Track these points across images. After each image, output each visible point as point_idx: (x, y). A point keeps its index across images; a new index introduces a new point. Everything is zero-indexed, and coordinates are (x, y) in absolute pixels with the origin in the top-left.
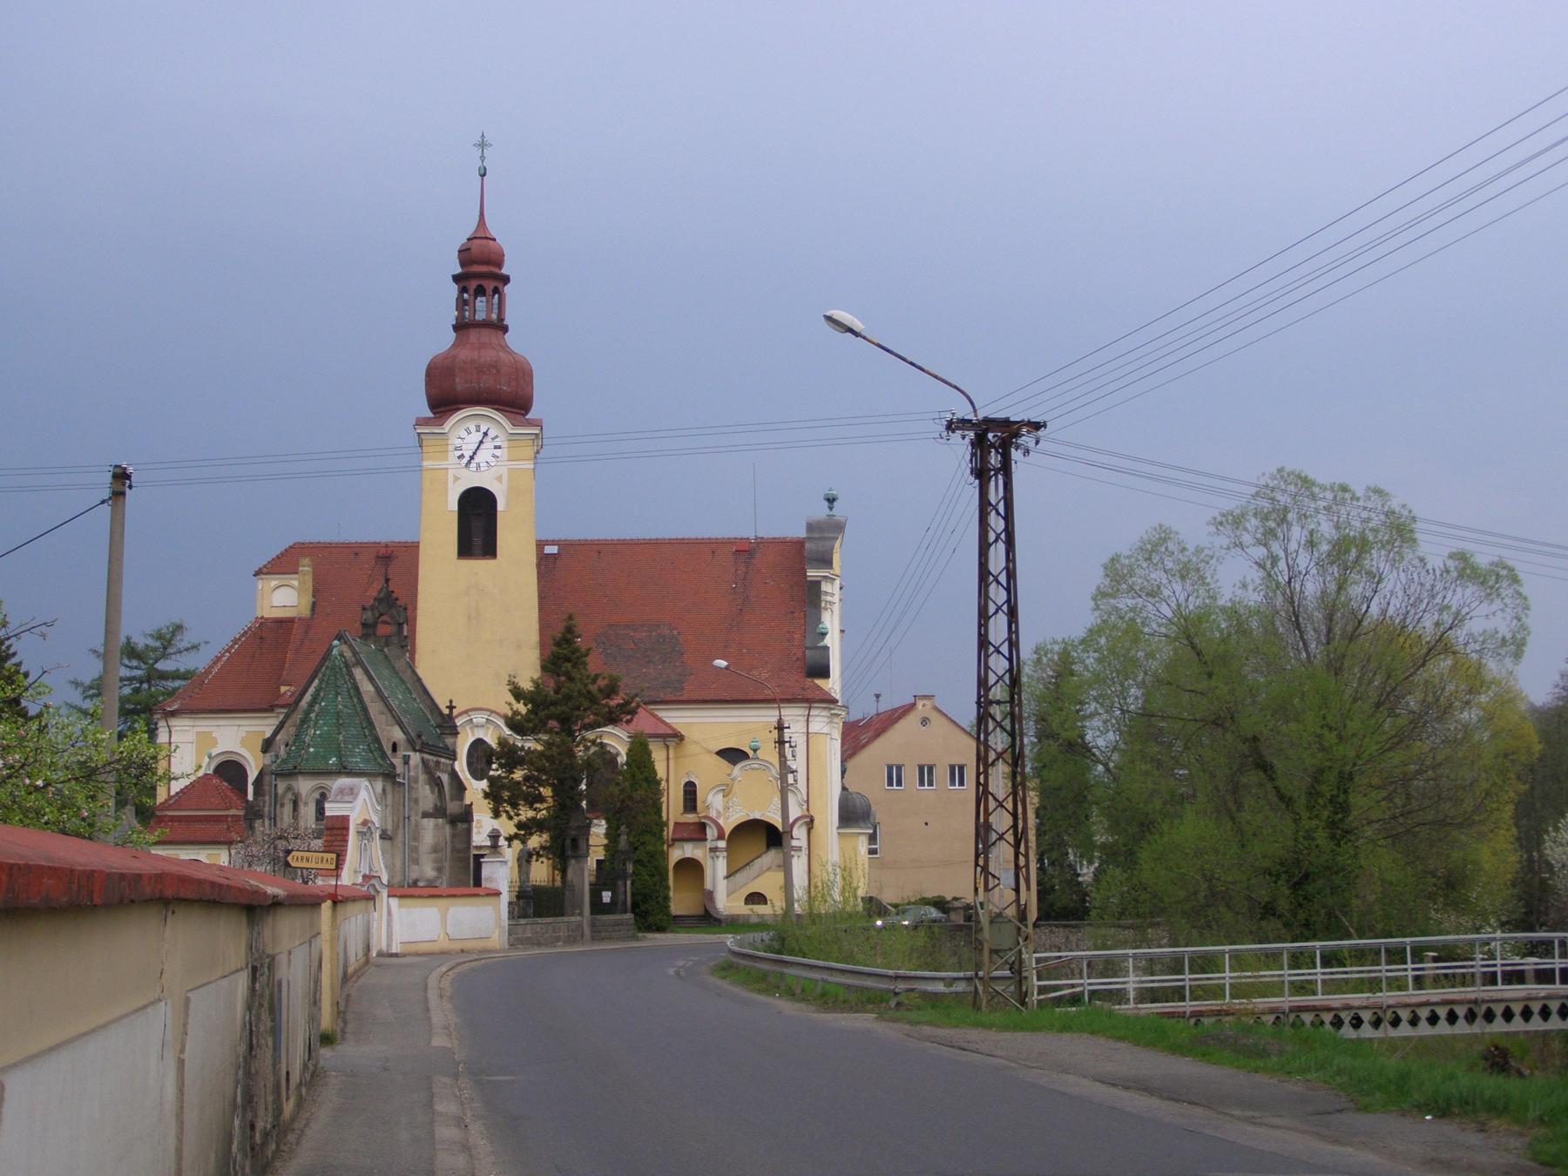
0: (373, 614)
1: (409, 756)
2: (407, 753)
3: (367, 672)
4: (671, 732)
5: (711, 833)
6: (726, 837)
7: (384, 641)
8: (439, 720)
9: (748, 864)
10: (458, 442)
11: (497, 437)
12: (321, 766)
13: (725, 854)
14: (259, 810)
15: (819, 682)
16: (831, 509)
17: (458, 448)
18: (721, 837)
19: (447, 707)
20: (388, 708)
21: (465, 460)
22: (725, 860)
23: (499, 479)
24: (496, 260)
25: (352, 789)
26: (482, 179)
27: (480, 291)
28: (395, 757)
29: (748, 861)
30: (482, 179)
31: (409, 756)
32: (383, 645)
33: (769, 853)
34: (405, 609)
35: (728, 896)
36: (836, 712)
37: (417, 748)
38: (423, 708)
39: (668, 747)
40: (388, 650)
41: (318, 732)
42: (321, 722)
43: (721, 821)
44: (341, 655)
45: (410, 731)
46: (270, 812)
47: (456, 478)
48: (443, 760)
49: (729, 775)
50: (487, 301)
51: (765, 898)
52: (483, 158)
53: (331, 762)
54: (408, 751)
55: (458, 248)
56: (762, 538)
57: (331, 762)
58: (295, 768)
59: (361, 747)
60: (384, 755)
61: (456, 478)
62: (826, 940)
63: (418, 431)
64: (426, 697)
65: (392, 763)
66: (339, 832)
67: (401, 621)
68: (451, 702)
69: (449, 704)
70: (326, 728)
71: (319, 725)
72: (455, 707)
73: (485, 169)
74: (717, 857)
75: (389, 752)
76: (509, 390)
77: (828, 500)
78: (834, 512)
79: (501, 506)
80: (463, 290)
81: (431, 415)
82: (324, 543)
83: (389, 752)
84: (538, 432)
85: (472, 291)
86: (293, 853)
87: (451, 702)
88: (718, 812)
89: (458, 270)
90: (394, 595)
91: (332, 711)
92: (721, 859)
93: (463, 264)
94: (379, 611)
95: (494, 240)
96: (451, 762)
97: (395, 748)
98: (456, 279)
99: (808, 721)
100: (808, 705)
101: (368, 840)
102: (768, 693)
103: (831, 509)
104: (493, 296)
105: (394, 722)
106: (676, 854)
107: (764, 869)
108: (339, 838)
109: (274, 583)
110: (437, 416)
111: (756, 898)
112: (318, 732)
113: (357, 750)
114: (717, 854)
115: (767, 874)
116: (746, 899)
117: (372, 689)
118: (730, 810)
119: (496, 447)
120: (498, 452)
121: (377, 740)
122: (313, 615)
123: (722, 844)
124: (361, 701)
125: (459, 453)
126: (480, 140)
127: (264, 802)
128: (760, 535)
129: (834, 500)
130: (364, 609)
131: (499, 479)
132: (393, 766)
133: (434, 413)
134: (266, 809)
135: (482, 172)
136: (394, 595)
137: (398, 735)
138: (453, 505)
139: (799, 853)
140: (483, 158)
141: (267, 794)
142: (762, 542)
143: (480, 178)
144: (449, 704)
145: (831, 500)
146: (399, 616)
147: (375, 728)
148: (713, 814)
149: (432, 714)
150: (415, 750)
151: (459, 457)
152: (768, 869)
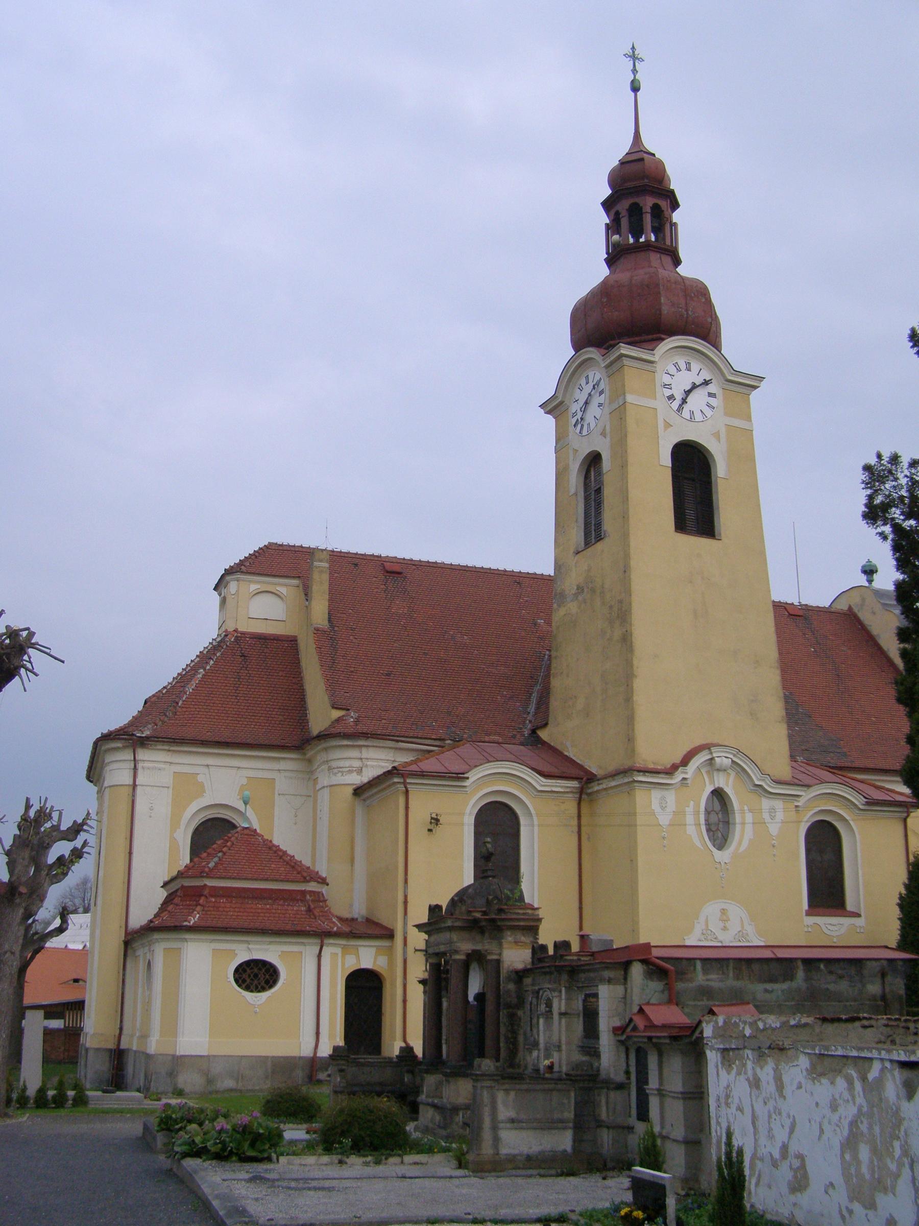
10: (667, 379)
21: (675, 405)
23: (717, 435)
47: (668, 425)
52: (634, 71)
109: (254, 587)
120: (712, 401)
140: (634, 71)
143: (632, 94)
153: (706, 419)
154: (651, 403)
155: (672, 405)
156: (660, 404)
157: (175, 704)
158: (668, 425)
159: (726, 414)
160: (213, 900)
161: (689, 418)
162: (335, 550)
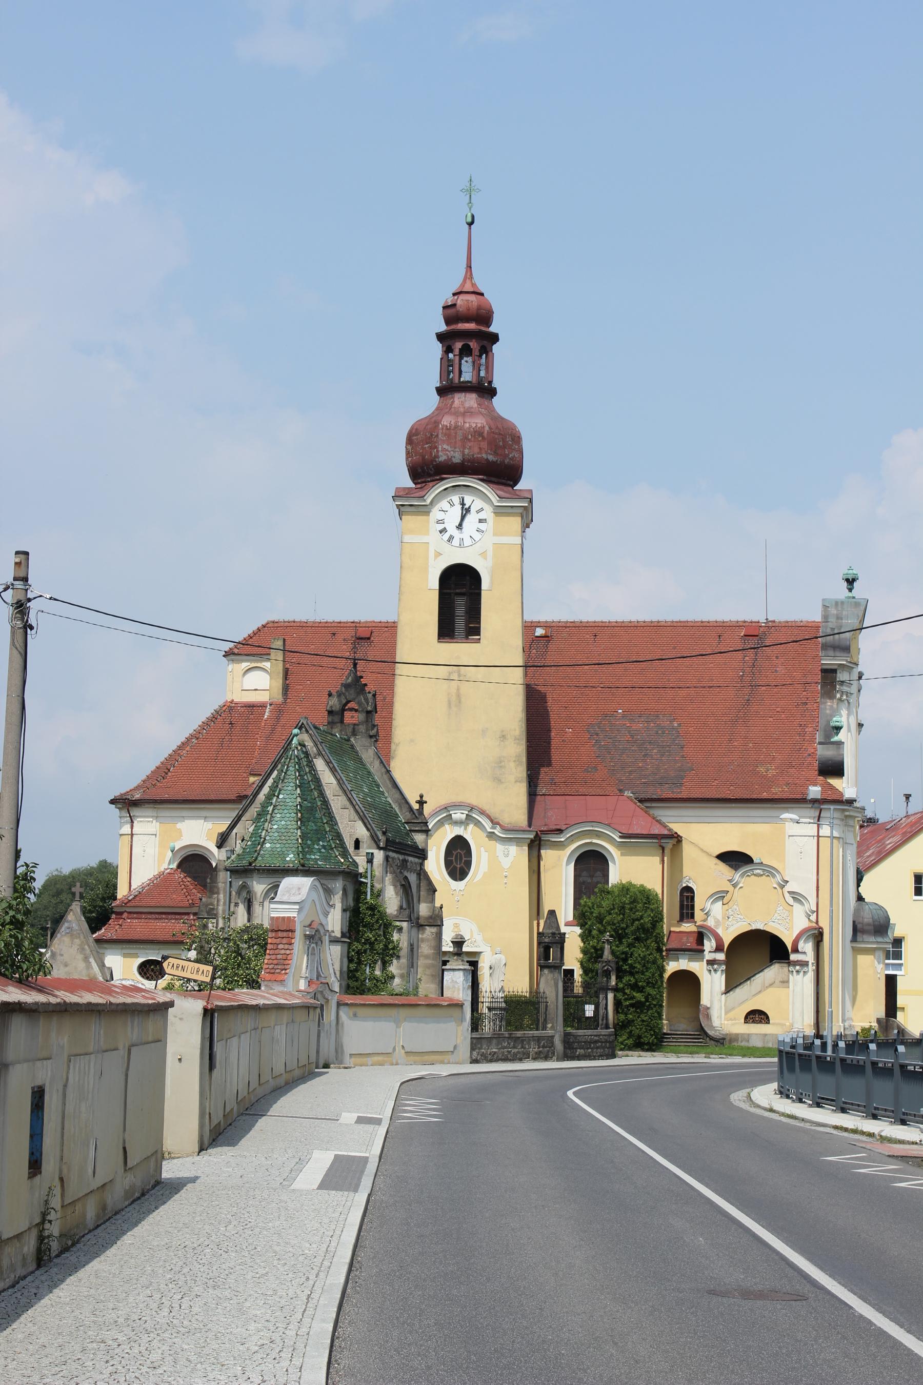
0: (340, 701)
1: (372, 854)
2: (371, 851)
3: (328, 763)
4: (666, 832)
5: (709, 945)
6: (725, 950)
7: (351, 730)
8: (408, 815)
9: (749, 979)
10: (440, 516)
11: (482, 509)
12: (277, 863)
13: (724, 967)
14: (213, 909)
15: (834, 782)
16: (850, 590)
17: (439, 522)
18: (719, 949)
19: (417, 802)
20: (351, 803)
22: (724, 976)
23: (483, 554)
24: (484, 317)
25: (299, 889)
26: (470, 228)
27: (466, 351)
28: (357, 855)
30: (470, 228)
31: (372, 854)
32: (349, 734)
33: (772, 967)
34: (374, 695)
35: (726, 1013)
36: (852, 814)
37: (382, 845)
38: (391, 802)
39: (663, 849)
40: (355, 739)
41: (275, 827)
42: (278, 815)
43: (720, 931)
44: (302, 745)
45: (373, 825)
46: (224, 911)
48: (410, 859)
49: (730, 881)
50: (474, 362)
51: (768, 1017)
53: (288, 859)
54: (370, 848)
55: (442, 304)
56: (774, 622)
57: (288, 859)
58: (250, 864)
59: (321, 843)
60: (345, 853)
61: (438, 554)
63: (397, 503)
64: (394, 790)
65: (354, 861)
66: (285, 934)
67: (369, 708)
68: (421, 796)
69: (419, 799)
70: (283, 823)
71: (276, 819)
72: (426, 802)
73: (473, 217)
74: (715, 971)
75: (351, 848)
76: (495, 459)
77: (847, 580)
78: (854, 593)
79: (485, 585)
80: (448, 350)
81: (412, 485)
82: (300, 622)
83: (351, 848)
84: (527, 505)
85: (457, 352)
86: (170, 960)
87: (421, 796)
88: (718, 922)
89: (443, 327)
90: (363, 681)
91: (291, 804)
92: (719, 973)
93: (448, 321)
94: (346, 698)
95: (482, 294)
96: (420, 861)
97: (357, 845)
98: (441, 337)
101: (316, 943)
102: (776, 791)
103: (850, 590)
104: (480, 356)
105: (357, 818)
106: (672, 967)
107: (767, 985)
108: (285, 941)
109: (245, 665)
110: (419, 486)
111: (757, 1016)
112: (275, 827)
113: (316, 847)
114: (715, 966)
115: (770, 989)
116: (746, 1017)
117: (334, 781)
118: (730, 920)
119: (481, 521)
120: (482, 526)
121: (339, 836)
122: (285, 699)
123: (721, 956)
124: (322, 794)
125: (441, 527)
126: (468, 185)
127: (218, 901)
128: (770, 619)
129: (854, 580)
130: (330, 695)
131: (483, 554)
132: (355, 864)
133: (415, 484)
134: (220, 908)
135: (469, 220)
136: (363, 681)
137: (361, 831)
138: (435, 584)
139: (805, 969)
141: (221, 892)
142: (772, 626)
144: (419, 799)
145: (850, 582)
146: (368, 704)
147: (336, 824)
148: (711, 923)
149: (400, 807)
150: (380, 848)
151: (441, 532)
152: (771, 985)
153: (474, 542)
154: (425, 539)
155: (443, 537)
156: (434, 539)
157: (166, 771)
158: (438, 554)
159: (495, 534)
160: (129, 921)
161: (458, 546)
162: (322, 621)
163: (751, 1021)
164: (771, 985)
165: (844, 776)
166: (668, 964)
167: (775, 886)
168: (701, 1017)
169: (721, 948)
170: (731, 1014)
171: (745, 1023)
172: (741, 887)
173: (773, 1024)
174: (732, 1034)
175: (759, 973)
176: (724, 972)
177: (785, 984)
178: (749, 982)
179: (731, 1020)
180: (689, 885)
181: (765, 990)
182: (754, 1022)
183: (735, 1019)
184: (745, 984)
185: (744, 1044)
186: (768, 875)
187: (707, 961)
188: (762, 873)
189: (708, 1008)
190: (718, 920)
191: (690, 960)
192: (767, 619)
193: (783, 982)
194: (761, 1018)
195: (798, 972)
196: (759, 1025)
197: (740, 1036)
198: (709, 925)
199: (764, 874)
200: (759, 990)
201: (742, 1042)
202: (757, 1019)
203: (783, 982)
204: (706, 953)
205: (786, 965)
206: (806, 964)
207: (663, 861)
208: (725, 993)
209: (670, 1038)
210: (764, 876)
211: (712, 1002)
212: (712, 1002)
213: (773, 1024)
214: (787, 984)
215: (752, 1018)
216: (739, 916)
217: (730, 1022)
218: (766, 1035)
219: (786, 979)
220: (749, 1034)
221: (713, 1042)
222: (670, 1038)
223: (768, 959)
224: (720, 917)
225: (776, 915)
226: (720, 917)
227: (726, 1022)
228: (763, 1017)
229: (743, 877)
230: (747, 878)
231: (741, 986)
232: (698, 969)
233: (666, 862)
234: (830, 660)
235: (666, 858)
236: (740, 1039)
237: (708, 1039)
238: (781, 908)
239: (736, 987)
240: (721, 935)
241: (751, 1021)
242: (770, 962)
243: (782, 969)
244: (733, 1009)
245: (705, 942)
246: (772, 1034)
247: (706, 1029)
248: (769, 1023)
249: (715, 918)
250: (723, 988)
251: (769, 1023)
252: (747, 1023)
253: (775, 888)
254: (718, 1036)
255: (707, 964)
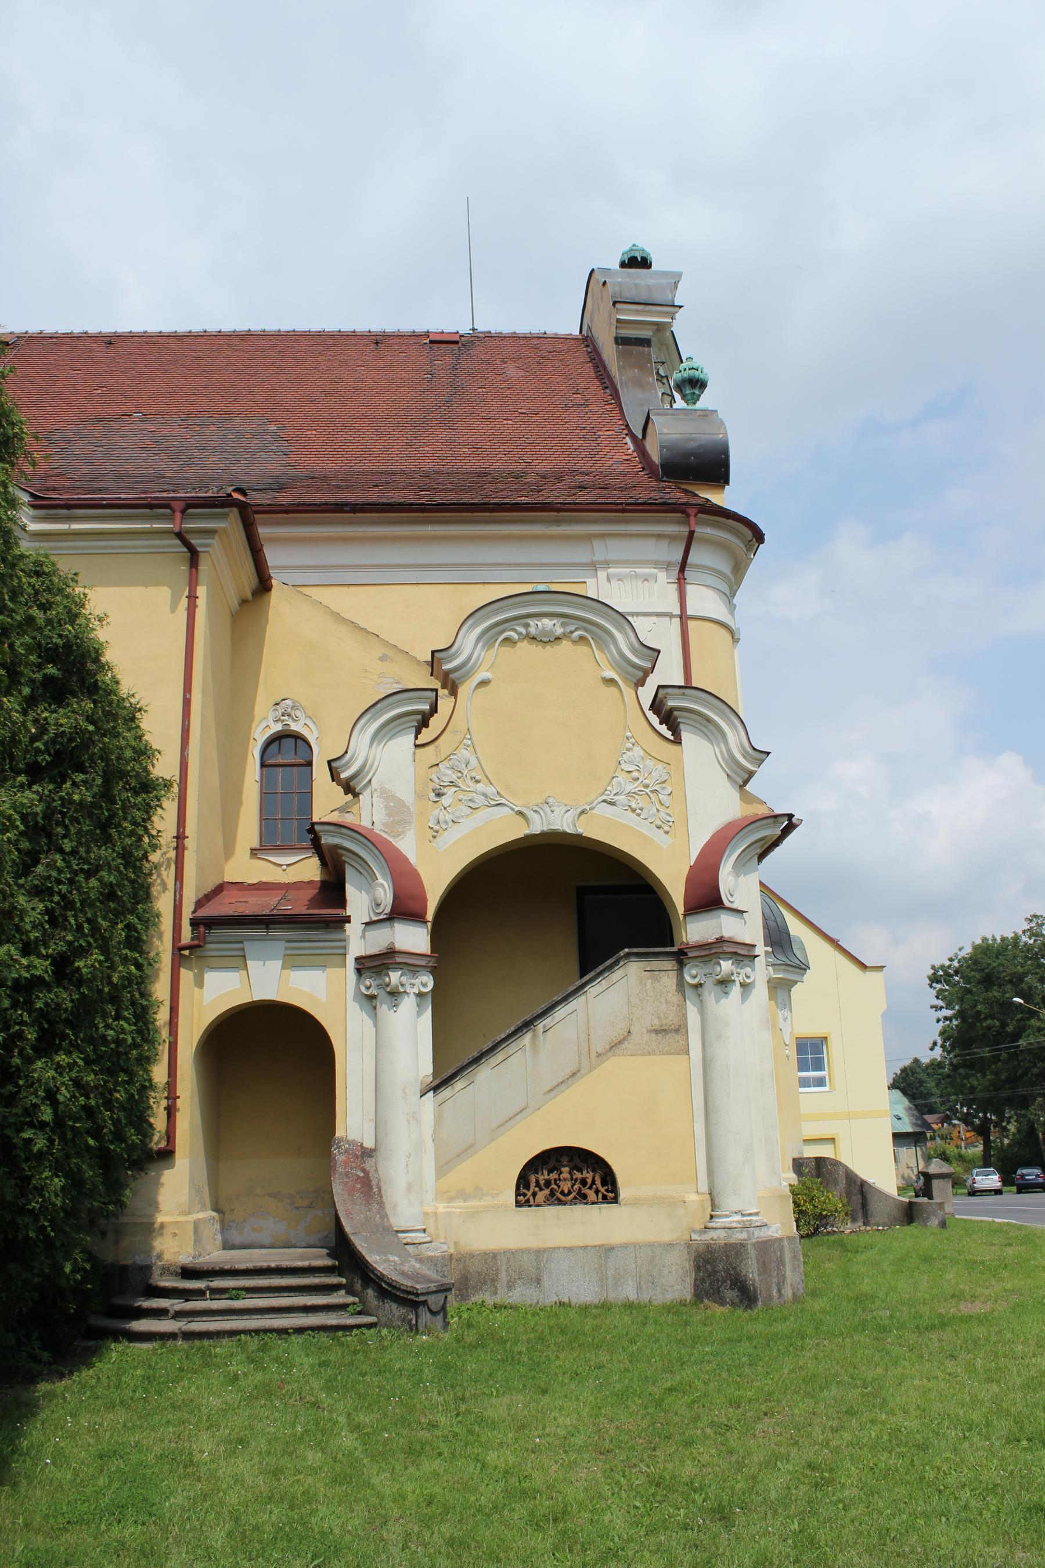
6: (430, 916)
9: (527, 1025)
13: (427, 982)
29: (528, 1017)
35: (442, 1169)
39: (194, 557)
43: (408, 846)
51: (609, 1178)
62: (830, 1316)
74: (395, 994)
88: (398, 811)
92: (408, 1003)
99: (682, 569)
100: (684, 530)
107: (599, 1046)
114: (395, 977)
115: (614, 1064)
116: (523, 1181)
118: (445, 801)
139: (741, 974)
152: (615, 1046)
163: (541, 1195)
164: (615, 1046)
165: (727, 482)
166: (200, 983)
167: (610, 674)
168: (338, 1189)
169: (414, 906)
170: (462, 1174)
171: (518, 1204)
172: (484, 683)
173: (636, 1202)
174: (472, 1256)
175: (565, 999)
176: (429, 998)
177: (672, 1039)
178: (527, 1039)
179: (462, 1195)
180: (294, 727)
181: (591, 1069)
182: (556, 1199)
183: (478, 1192)
184: (513, 1048)
185: (520, 1295)
186: (582, 638)
187: (358, 959)
188: (559, 631)
189: (368, 1153)
190: (401, 803)
191: (292, 961)
192: (473, 329)
193: (661, 1031)
194: (584, 1182)
195: (724, 983)
196: (579, 1211)
197: (502, 1263)
198: (366, 823)
199: (565, 636)
200: (568, 1071)
201: (510, 1287)
202: (566, 1186)
203: (661, 1031)
204: (353, 930)
205: (669, 964)
206: (743, 954)
207: (192, 597)
208: (436, 1089)
209: (199, 1294)
210: (565, 644)
211: (379, 1123)
212: (379, 1123)
213: (636, 1202)
214: (677, 1037)
215: (548, 1183)
216: (480, 787)
217: (459, 1206)
218: (607, 1250)
219: (671, 1019)
220: (538, 1253)
221: (394, 1310)
222: (199, 1294)
223: (575, 966)
224: (405, 792)
225: (622, 778)
226: (405, 792)
227: (442, 1208)
228: (588, 1175)
229: (489, 645)
230: (506, 650)
231: (499, 1056)
232: (323, 997)
233: (202, 602)
234: (637, 312)
235: (201, 591)
236: (503, 1277)
237: (370, 1293)
238: (637, 751)
239: (477, 1060)
240: (413, 860)
241: (541, 1195)
242: (583, 973)
243: (657, 980)
244: (468, 1150)
245: (351, 891)
246: (637, 1246)
247: (361, 1245)
248: (615, 1200)
249: (388, 796)
250: (425, 1067)
251: (615, 1200)
252: (527, 1203)
253: (611, 682)
254: (416, 1276)
255: (359, 971)
